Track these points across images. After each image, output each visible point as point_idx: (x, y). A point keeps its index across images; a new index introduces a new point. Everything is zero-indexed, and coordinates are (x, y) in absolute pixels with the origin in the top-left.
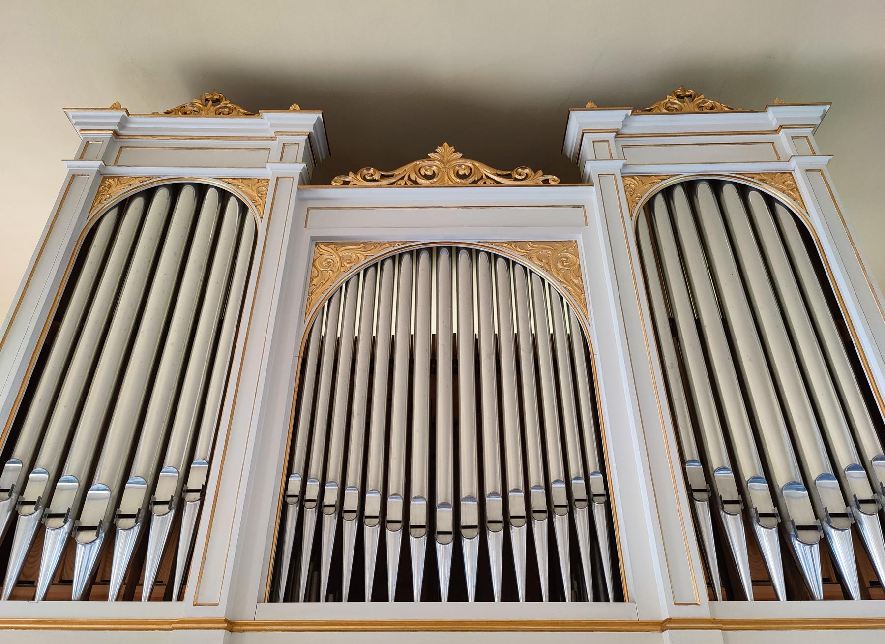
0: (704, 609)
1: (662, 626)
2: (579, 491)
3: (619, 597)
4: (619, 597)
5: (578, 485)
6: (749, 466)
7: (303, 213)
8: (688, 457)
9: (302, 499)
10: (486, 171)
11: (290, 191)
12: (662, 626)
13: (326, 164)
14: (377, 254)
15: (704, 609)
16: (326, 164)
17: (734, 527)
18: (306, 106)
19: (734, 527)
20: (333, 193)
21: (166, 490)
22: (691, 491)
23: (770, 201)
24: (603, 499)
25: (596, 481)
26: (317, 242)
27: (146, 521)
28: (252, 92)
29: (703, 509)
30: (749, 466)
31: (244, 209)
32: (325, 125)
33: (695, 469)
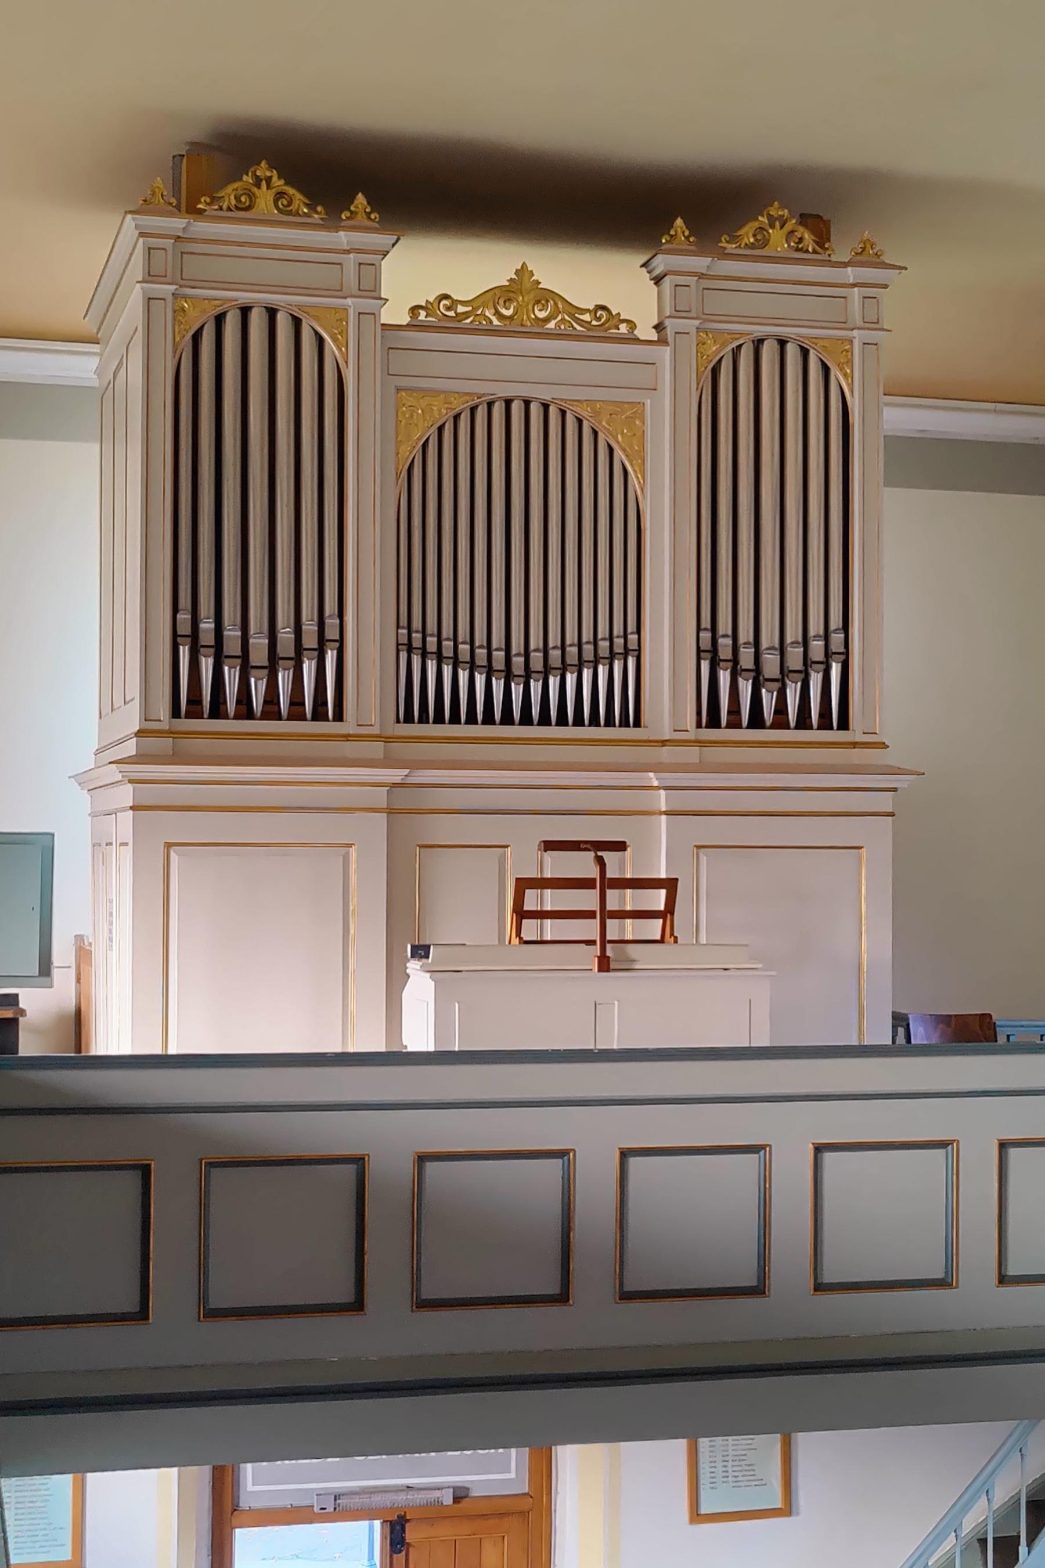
0: (692, 733)
1: (664, 743)
3: (637, 724)
4: (637, 724)
5: (619, 642)
6: (746, 634)
8: (703, 626)
12: (664, 743)
15: (692, 733)
17: (724, 678)
19: (724, 678)
22: (699, 651)
24: (636, 653)
25: (633, 638)
29: (705, 666)
30: (746, 634)
33: (706, 636)
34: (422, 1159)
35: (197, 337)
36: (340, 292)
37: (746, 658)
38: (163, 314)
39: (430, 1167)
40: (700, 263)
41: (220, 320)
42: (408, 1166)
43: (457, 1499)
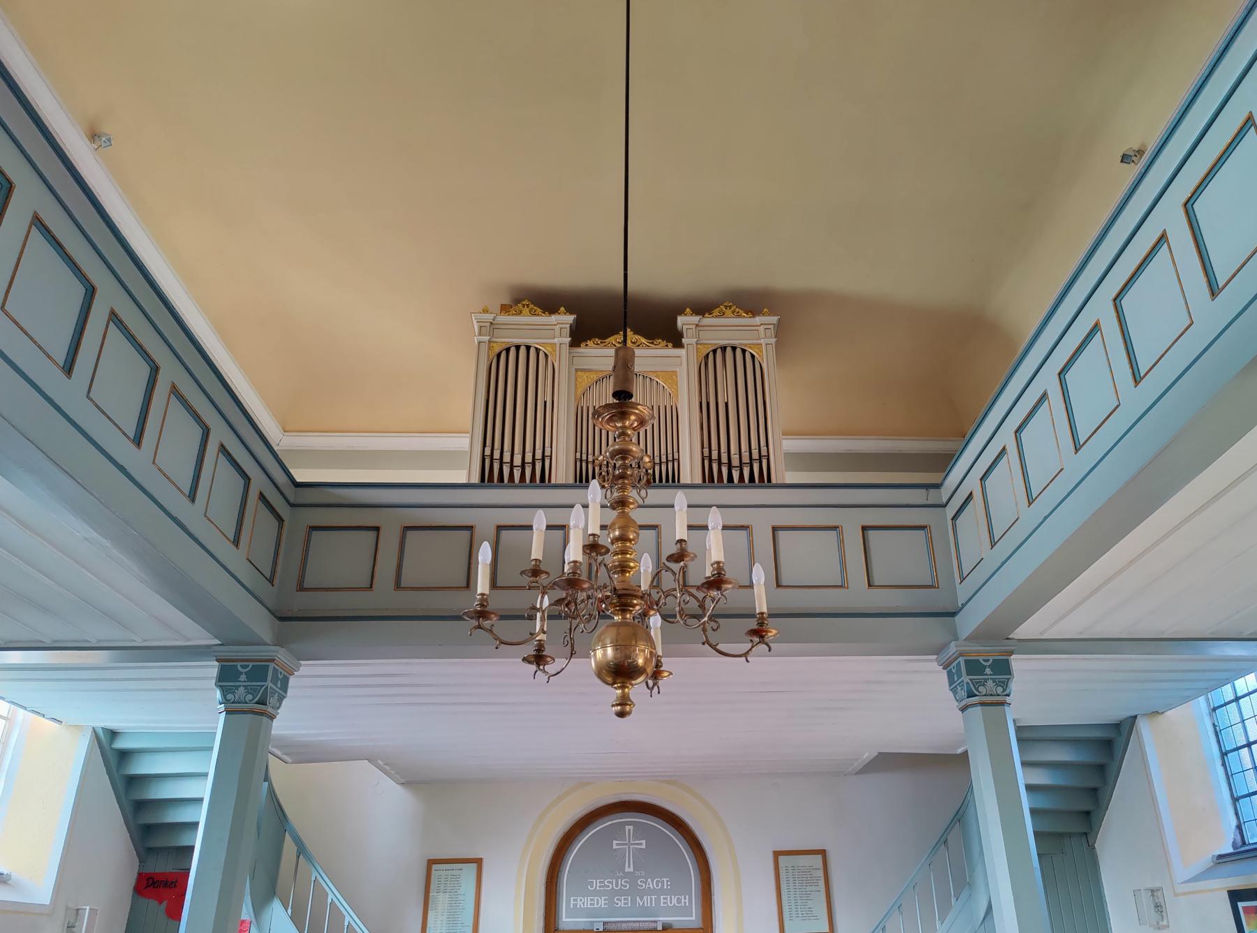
2: (670, 458)
7: (572, 358)
10: (643, 340)
11: (566, 348)
13: (579, 336)
14: (601, 375)
16: (579, 336)
18: (569, 311)
20: (582, 350)
21: (539, 455)
23: (753, 356)
26: (577, 370)
27: (533, 463)
28: (547, 301)
29: (706, 462)
31: (546, 355)
32: (577, 321)
34: (500, 528)
35: (499, 355)
37: (724, 459)
38: (484, 348)
39: (504, 533)
40: (696, 319)
41: (508, 350)
42: (493, 531)
43: (664, 928)
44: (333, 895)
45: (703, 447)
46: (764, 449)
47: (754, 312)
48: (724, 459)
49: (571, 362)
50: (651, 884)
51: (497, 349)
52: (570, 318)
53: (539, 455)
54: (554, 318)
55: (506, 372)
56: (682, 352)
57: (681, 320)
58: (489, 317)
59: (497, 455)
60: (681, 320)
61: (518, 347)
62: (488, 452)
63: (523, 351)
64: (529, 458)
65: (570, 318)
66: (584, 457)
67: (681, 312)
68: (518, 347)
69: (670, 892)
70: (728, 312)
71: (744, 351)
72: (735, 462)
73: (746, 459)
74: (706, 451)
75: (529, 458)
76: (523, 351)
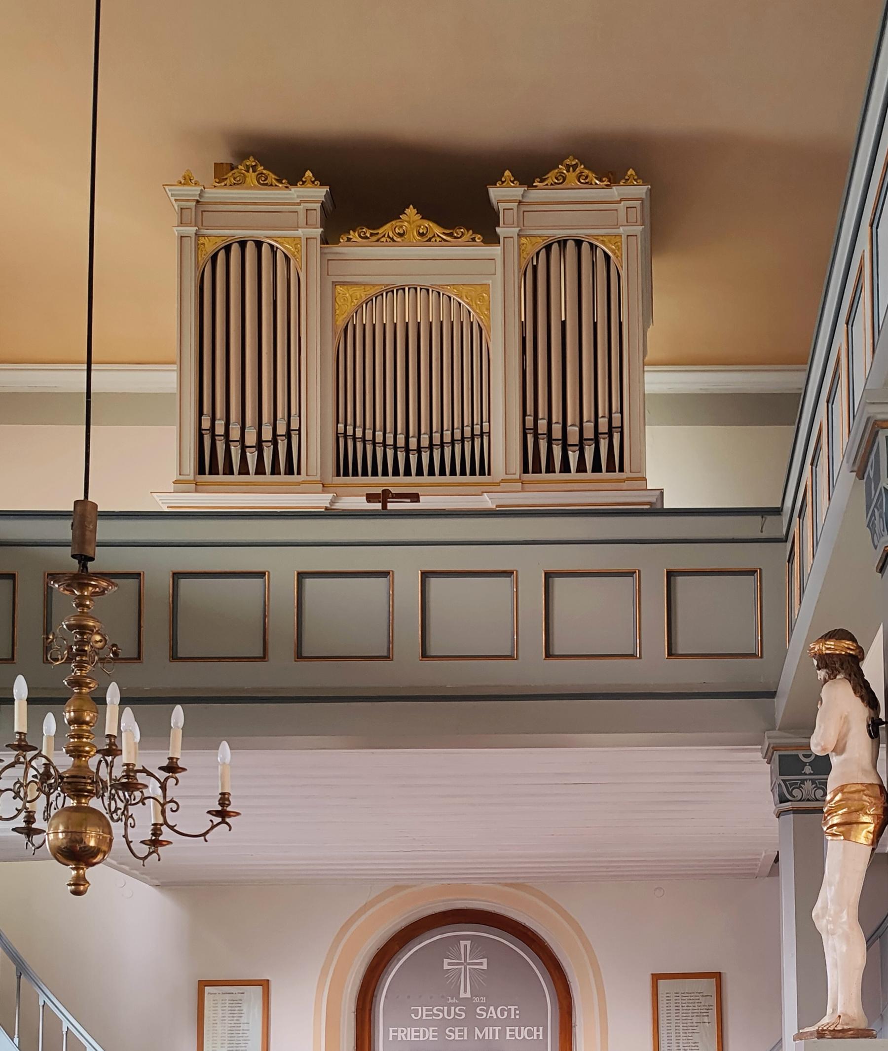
6: (556, 416)
7: (326, 261)
9: (345, 436)
10: (437, 230)
11: (316, 245)
13: (337, 221)
14: (373, 291)
16: (337, 221)
18: (321, 179)
20: (342, 249)
21: (281, 430)
23: (607, 257)
26: (335, 284)
27: (275, 442)
28: (280, 157)
31: (287, 259)
32: (331, 194)
35: (214, 258)
36: (296, 228)
37: (557, 433)
40: (517, 191)
41: (228, 249)
44: (68, 1022)
45: (524, 414)
46: (616, 416)
47: (613, 177)
48: (557, 433)
49: (325, 273)
50: (494, 1013)
51: (210, 248)
52: (321, 192)
53: (281, 430)
54: (295, 193)
55: (226, 289)
56: (495, 251)
57: (495, 193)
58: (193, 191)
59: (220, 430)
60: (495, 193)
61: (243, 244)
62: (206, 424)
63: (250, 248)
64: (267, 435)
65: (321, 192)
66: (350, 431)
67: (495, 179)
68: (243, 244)
69: (519, 1023)
70: (571, 176)
71: (593, 247)
72: (573, 438)
73: (589, 433)
74: (530, 420)
75: (267, 435)
76: (250, 248)
